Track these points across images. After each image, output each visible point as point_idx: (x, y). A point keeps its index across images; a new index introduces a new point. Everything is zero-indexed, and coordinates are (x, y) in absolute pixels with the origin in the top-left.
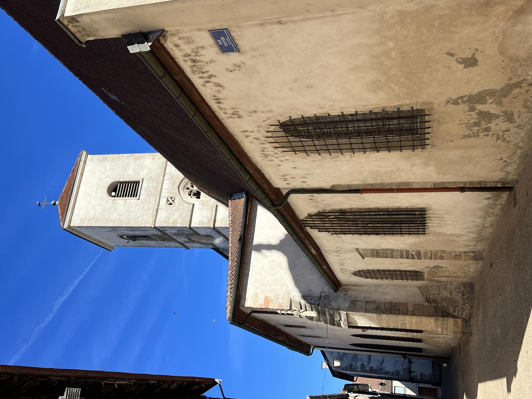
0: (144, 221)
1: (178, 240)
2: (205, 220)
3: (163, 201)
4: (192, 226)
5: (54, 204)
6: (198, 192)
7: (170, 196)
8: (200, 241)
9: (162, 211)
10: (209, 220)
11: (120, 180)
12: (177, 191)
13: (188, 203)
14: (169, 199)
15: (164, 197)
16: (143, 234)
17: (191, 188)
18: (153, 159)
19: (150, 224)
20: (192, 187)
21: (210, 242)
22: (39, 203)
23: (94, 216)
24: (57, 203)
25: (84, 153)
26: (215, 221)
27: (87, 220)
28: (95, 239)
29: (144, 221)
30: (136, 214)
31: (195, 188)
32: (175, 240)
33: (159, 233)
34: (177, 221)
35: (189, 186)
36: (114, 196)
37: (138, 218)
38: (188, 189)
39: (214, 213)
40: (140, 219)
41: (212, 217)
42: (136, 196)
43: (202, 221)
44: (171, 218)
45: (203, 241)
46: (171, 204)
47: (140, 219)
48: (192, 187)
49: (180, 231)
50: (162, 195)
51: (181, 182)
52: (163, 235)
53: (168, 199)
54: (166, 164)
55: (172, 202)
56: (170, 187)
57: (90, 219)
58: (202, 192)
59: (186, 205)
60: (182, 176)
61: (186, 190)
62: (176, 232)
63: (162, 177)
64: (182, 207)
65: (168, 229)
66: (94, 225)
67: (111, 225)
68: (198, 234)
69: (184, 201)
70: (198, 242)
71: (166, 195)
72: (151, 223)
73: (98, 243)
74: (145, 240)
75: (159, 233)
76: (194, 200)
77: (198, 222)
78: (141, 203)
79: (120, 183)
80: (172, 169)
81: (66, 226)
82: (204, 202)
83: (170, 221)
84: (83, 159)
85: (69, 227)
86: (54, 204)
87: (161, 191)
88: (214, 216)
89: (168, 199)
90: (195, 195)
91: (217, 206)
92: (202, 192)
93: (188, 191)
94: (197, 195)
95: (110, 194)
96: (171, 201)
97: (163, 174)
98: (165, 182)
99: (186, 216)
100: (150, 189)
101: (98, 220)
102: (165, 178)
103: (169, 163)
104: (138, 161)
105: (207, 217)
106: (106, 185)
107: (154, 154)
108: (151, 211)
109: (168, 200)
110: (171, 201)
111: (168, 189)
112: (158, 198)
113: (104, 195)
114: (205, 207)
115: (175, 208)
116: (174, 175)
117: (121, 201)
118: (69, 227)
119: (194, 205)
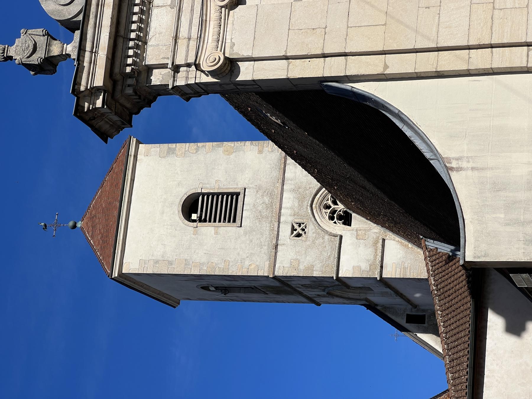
0: (253, 267)
2: (365, 266)
3: (285, 231)
4: (340, 276)
5: (74, 226)
6: (345, 212)
7: (297, 221)
8: (346, 296)
9: (283, 247)
10: (370, 265)
11: (203, 191)
12: (310, 211)
14: (296, 226)
15: (286, 222)
16: (247, 284)
17: (333, 206)
18: (260, 152)
19: (264, 272)
22: (45, 225)
23: (163, 257)
24: (79, 225)
25: (134, 141)
26: (382, 267)
27: (152, 263)
29: (253, 267)
30: (239, 254)
31: (340, 207)
33: (277, 284)
34: (313, 266)
35: (330, 202)
36: (194, 221)
37: (243, 260)
38: (327, 207)
39: (380, 254)
40: (247, 263)
41: (375, 259)
42: (234, 221)
43: (359, 267)
46: (299, 235)
47: (247, 263)
50: (282, 219)
51: (316, 195)
53: (293, 227)
54: (285, 161)
55: (301, 232)
56: (296, 205)
58: (354, 215)
59: (327, 237)
60: (315, 184)
61: (324, 210)
63: (279, 185)
64: (321, 240)
66: (165, 271)
69: (323, 230)
70: (341, 297)
71: (290, 219)
72: (266, 269)
75: (277, 284)
76: (339, 228)
77: (351, 269)
78: (245, 233)
79: (203, 195)
80: (296, 172)
81: (116, 274)
82: (360, 232)
83: (302, 267)
85: (121, 274)
86: (74, 226)
88: (379, 258)
89: (293, 227)
90: (340, 218)
91: (384, 240)
92: (354, 215)
93: (329, 211)
94: (346, 220)
95: (188, 217)
96: (299, 230)
97: (280, 181)
98: (285, 195)
99: (329, 257)
100: (260, 208)
101: (170, 263)
103: (290, 160)
104: (232, 156)
105: (368, 261)
106: (178, 200)
108: (266, 248)
109: (293, 229)
111: (292, 208)
112: (276, 225)
113: (177, 218)
115: (308, 243)
117: (208, 230)
118: (121, 274)
119: (341, 237)
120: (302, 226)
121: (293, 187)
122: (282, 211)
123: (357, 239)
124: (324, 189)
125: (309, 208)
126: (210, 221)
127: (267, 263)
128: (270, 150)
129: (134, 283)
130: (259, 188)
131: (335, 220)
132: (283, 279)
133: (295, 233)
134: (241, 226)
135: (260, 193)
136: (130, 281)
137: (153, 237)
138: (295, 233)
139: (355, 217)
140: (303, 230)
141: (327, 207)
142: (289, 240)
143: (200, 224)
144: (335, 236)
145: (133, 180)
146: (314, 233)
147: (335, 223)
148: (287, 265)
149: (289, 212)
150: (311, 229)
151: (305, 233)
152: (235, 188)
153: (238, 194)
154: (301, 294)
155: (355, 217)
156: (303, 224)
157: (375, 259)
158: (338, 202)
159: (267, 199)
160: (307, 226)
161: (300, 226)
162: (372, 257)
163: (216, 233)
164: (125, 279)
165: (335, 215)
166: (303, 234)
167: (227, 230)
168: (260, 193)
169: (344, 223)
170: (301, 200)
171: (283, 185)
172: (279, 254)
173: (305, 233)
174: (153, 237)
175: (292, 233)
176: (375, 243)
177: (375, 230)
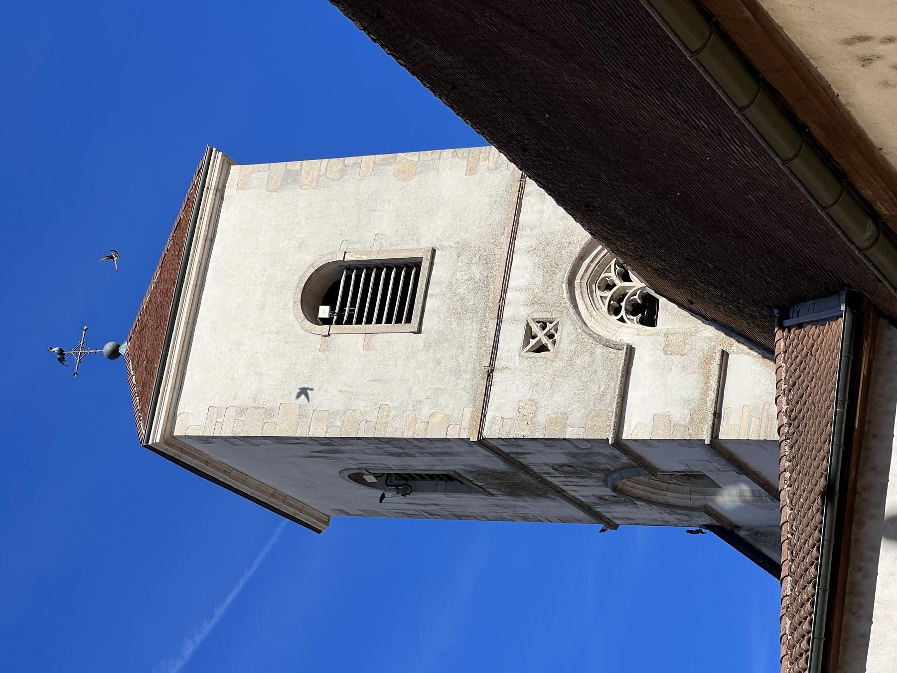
0: (438, 418)
1: (571, 491)
3: (512, 337)
5: (115, 353)
6: (646, 297)
8: (659, 498)
10: (693, 413)
11: (348, 258)
12: (566, 295)
13: (608, 344)
14: (536, 329)
15: (514, 320)
16: (439, 466)
17: (619, 284)
18: (471, 171)
19: (463, 430)
20: (625, 277)
21: (698, 500)
22: (61, 352)
23: (255, 399)
24: (123, 350)
25: (218, 158)
26: (717, 415)
27: (232, 412)
28: (261, 486)
29: (438, 418)
31: (637, 284)
32: (560, 493)
33: (498, 465)
34: (565, 415)
35: (613, 276)
36: (327, 321)
38: (609, 287)
39: (714, 384)
40: (426, 411)
42: (409, 320)
43: (667, 417)
44: (544, 402)
45: (671, 497)
46: (542, 348)
47: (426, 411)
48: (625, 277)
49: (580, 457)
51: (581, 258)
52: (510, 471)
53: (529, 328)
54: (521, 189)
55: (545, 340)
56: (539, 281)
57: (242, 411)
58: (662, 300)
59: (600, 350)
60: (580, 235)
61: (599, 293)
62: (564, 460)
63: (505, 240)
64: (587, 358)
65: (530, 447)
67: (318, 431)
68: (652, 470)
70: (650, 502)
72: (465, 424)
73: (274, 502)
74: (445, 491)
75: (498, 465)
76: (630, 331)
78: (427, 346)
80: (543, 210)
81: (156, 437)
83: (541, 418)
84: (213, 180)
86: (115, 353)
87: (503, 298)
88: (712, 396)
90: (634, 310)
91: (725, 355)
92: (662, 300)
93: (609, 294)
94: (646, 312)
95: (311, 315)
97: (508, 230)
99: (603, 395)
100: (462, 290)
101: (269, 413)
102: (517, 243)
103: (531, 186)
104: (413, 182)
106: (296, 279)
107: (475, 150)
108: (468, 376)
109: (530, 334)
110: (541, 335)
111: (528, 289)
113: (291, 317)
114: (676, 358)
115: (559, 364)
116: (553, 233)
117: (350, 339)
118: (169, 438)
119: (631, 351)
120: (549, 326)
121: (533, 242)
122: (509, 295)
123: (666, 353)
124: (606, 251)
125: (565, 286)
126: (359, 322)
127: (468, 411)
128: (492, 166)
129: (207, 463)
130: (462, 248)
131: (623, 313)
132: (506, 450)
133: (533, 342)
134: (419, 331)
135: (465, 258)
136: (195, 457)
137: (245, 363)
138: (533, 342)
139: (667, 309)
140: (551, 336)
141: (609, 287)
142: (518, 358)
143: (334, 328)
144: (617, 347)
145: (210, 240)
146: (572, 342)
147: (622, 320)
148: (510, 413)
149: (522, 296)
150: (566, 334)
151: (554, 343)
152: (413, 250)
153: (416, 264)
154: (560, 493)
155: (667, 309)
156: (551, 323)
157: (704, 398)
158: (631, 276)
159: (477, 271)
160: (560, 328)
161: (544, 328)
162: (697, 394)
163: (367, 347)
164: (182, 450)
165: (623, 304)
166: (550, 346)
167: (389, 338)
168: (465, 258)
169: (642, 322)
170: (549, 270)
171: (513, 238)
172: (494, 389)
173: (554, 343)
174: (245, 363)
175: (526, 343)
176: (707, 361)
177: (709, 336)
